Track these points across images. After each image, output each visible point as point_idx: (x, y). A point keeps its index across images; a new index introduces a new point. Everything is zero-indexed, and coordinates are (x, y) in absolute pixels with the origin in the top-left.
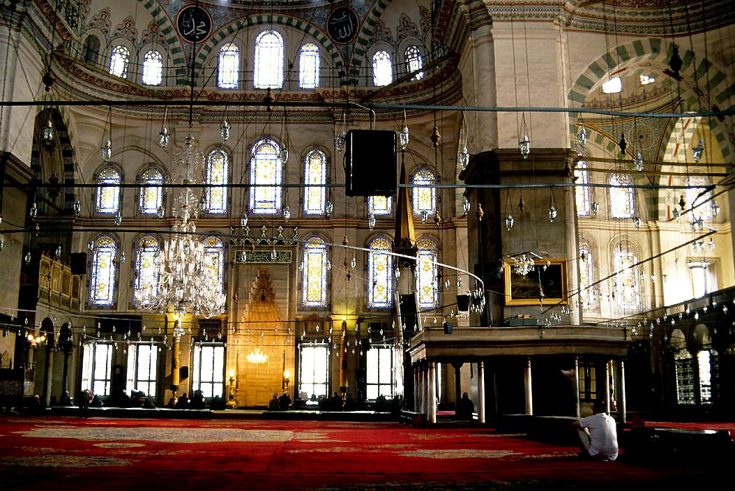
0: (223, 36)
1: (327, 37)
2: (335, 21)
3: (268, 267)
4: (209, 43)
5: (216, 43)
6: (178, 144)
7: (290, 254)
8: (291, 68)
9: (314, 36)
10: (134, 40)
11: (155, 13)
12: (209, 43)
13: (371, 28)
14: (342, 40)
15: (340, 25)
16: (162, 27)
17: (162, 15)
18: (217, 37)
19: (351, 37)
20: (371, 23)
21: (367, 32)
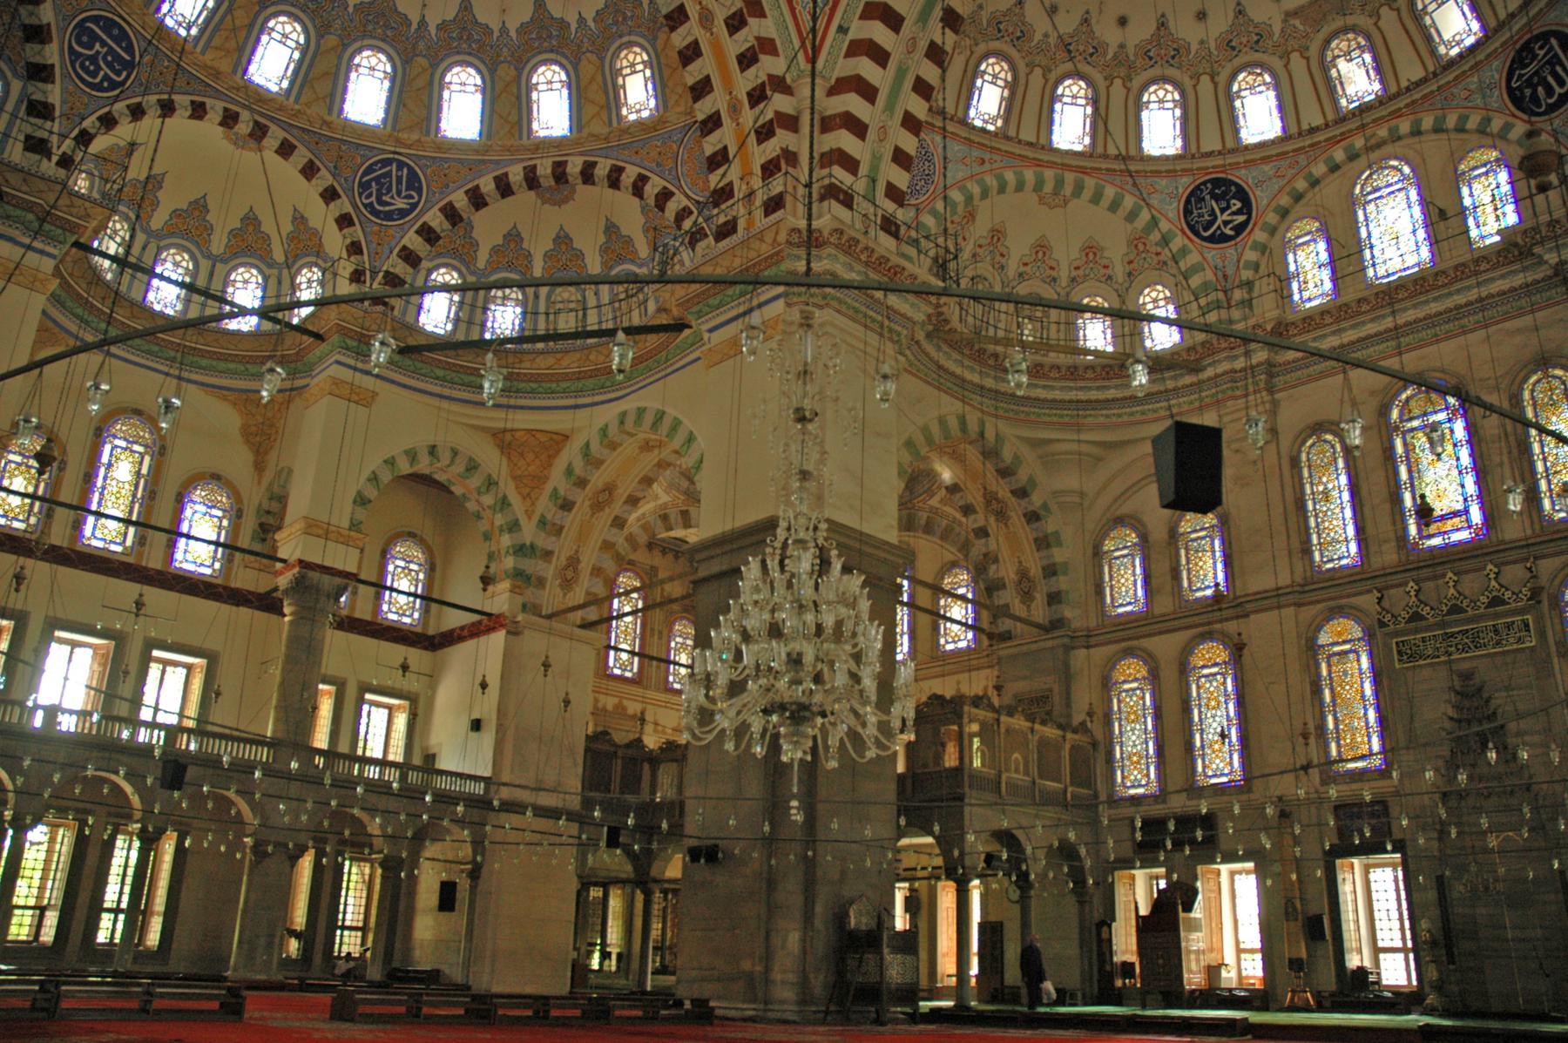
0: (1284, 213)
1: (1510, 119)
3: (1475, 663)
5: (1273, 231)
7: (1527, 625)
8: (1443, 217)
9: (1482, 131)
18: (1272, 218)
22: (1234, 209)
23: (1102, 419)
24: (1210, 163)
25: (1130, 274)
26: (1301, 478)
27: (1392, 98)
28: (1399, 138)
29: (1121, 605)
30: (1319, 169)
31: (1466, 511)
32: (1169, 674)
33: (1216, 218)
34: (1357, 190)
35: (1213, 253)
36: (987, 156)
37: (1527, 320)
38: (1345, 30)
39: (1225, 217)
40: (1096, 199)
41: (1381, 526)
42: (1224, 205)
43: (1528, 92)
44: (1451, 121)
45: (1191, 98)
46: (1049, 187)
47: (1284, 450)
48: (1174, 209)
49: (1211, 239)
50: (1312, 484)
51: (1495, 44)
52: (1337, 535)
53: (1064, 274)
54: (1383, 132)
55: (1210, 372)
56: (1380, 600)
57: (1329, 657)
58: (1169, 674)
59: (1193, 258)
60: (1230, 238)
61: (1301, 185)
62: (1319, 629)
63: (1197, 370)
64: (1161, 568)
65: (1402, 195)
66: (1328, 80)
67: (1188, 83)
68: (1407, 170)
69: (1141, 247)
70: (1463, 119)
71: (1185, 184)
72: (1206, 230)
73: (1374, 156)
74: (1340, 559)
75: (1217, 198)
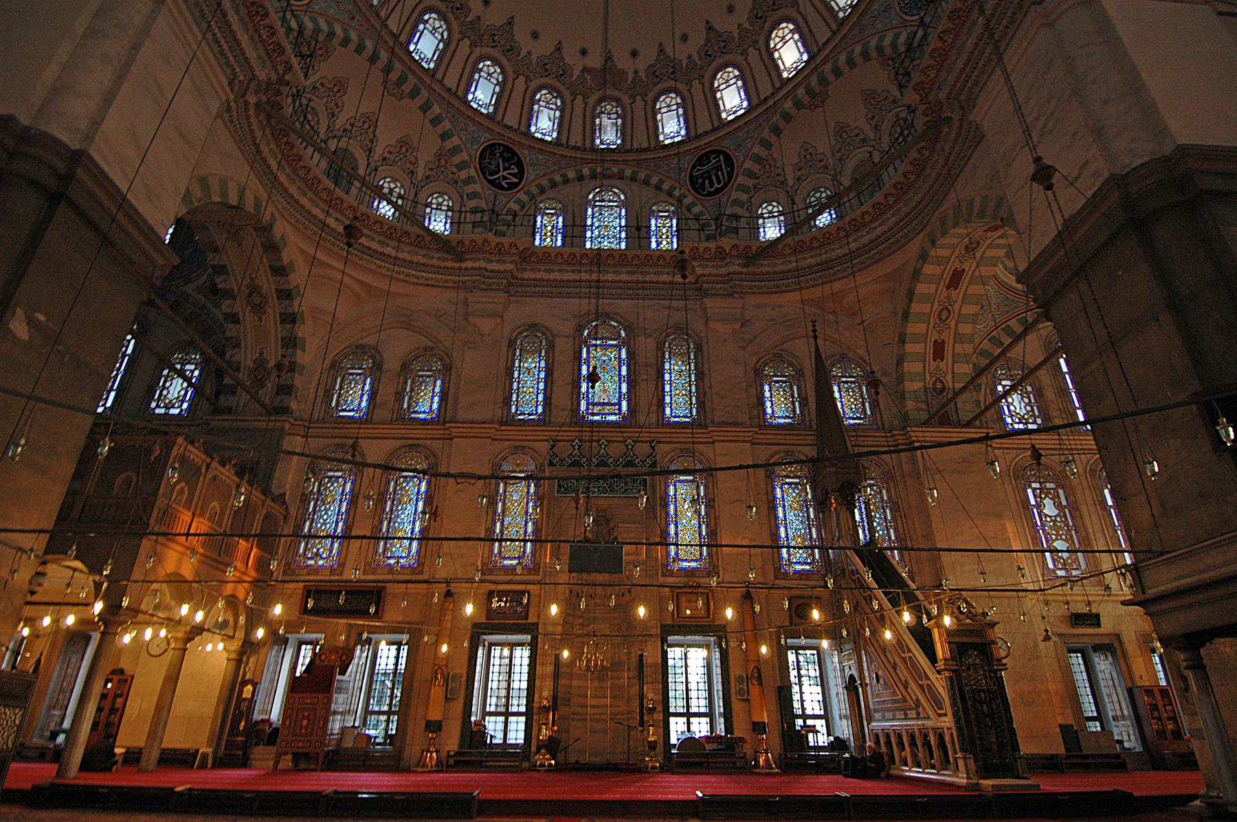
0: (542, 190)
4: (523, 197)
5: (532, 197)
6: (471, 319)
8: (638, 230)
9: (669, 193)
10: (412, 172)
11: (445, 136)
12: (523, 197)
13: (756, 168)
14: (710, 194)
16: (456, 159)
17: (455, 141)
18: (534, 190)
19: (726, 185)
20: (758, 159)
21: (749, 174)
23: (374, 267)
24: (508, 134)
28: (622, 178)
29: (344, 410)
30: (571, 174)
31: (619, 404)
34: (591, 197)
35: (490, 192)
36: (358, 17)
41: (561, 399)
44: (654, 180)
45: (509, 86)
47: (507, 331)
48: (476, 150)
49: (492, 183)
54: (615, 170)
55: (469, 264)
56: (553, 447)
60: (502, 188)
61: (558, 178)
64: (387, 390)
67: (511, 75)
68: (622, 197)
69: (443, 162)
71: (485, 138)
72: (491, 175)
73: (606, 182)
74: (530, 414)
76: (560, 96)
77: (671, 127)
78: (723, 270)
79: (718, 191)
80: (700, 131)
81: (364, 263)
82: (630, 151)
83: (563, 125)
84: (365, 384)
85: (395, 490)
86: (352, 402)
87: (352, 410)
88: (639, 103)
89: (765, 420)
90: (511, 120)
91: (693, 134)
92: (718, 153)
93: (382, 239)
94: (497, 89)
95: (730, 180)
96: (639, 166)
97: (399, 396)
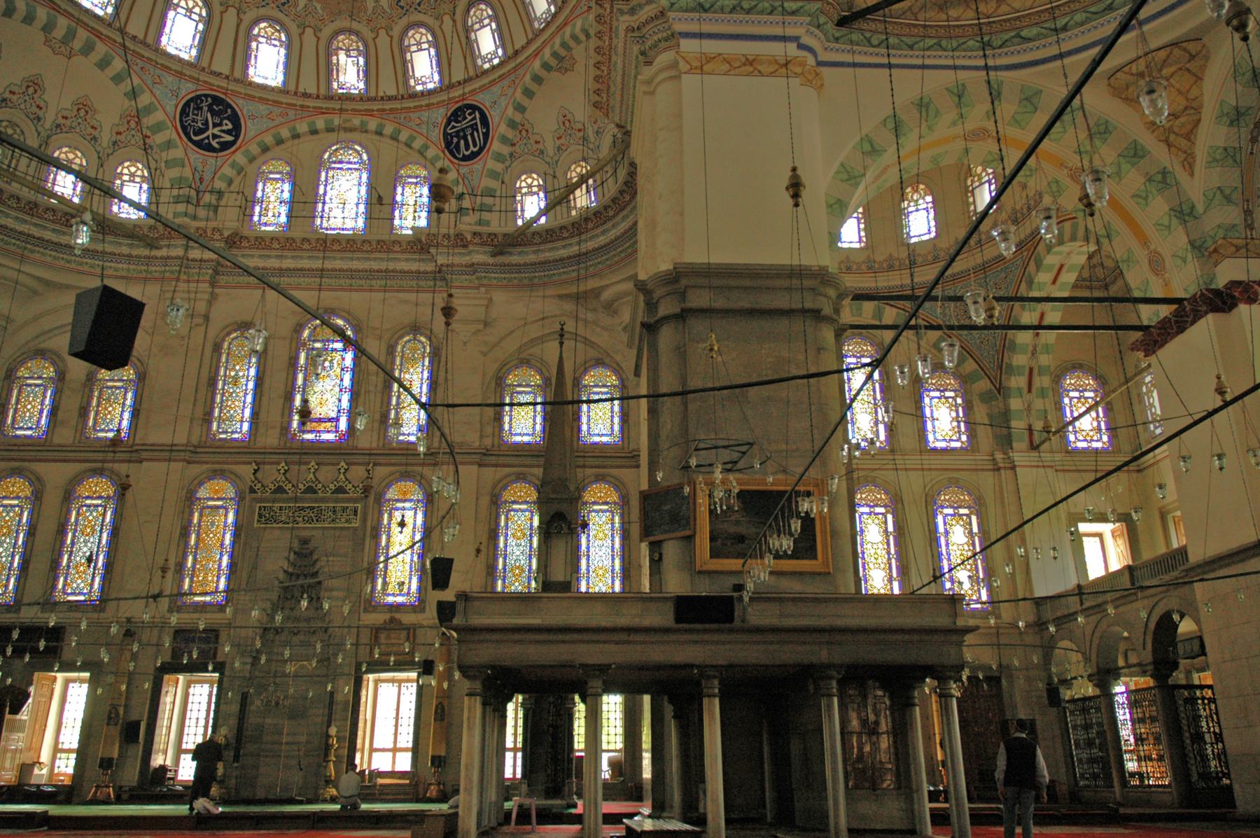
0: (265, 149)
2: (454, 127)
3: (314, 533)
7: (356, 511)
9: (421, 153)
13: (510, 134)
14: (465, 158)
15: (461, 134)
18: (254, 149)
19: (482, 149)
20: (512, 124)
22: (225, 128)
24: (215, 81)
25: (115, 143)
26: (219, 361)
27: (369, 99)
28: (366, 131)
30: (302, 127)
31: (337, 419)
32: (52, 498)
33: (207, 129)
34: (326, 156)
35: (196, 156)
37: (412, 297)
38: (350, 31)
39: (216, 131)
40: (103, 64)
41: (272, 414)
42: (217, 121)
43: (455, 140)
44: (404, 136)
46: (59, 33)
47: (212, 333)
49: (199, 144)
50: (226, 368)
51: (444, 97)
52: (236, 414)
53: (50, 119)
54: (356, 121)
55: (163, 252)
56: (256, 471)
57: (203, 508)
58: (52, 498)
59: (177, 153)
61: (285, 133)
62: (201, 484)
63: (152, 246)
64: (71, 404)
65: (356, 174)
66: (329, 62)
68: (365, 157)
70: (412, 138)
71: (188, 90)
72: (196, 135)
73: (343, 135)
75: (213, 113)
76: (284, 28)
77: (423, 68)
78: (466, 260)
79: (474, 155)
80: (454, 80)
81: (37, 256)
82: (375, 99)
83: (292, 66)
84: (45, 397)
85: (77, 520)
86: (30, 417)
87: (30, 428)
88: (383, 38)
89: (501, 437)
90: (222, 65)
91: (447, 82)
92: (474, 108)
93: (57, 227)
94: (201, 27)
95: (485, 143)
96: (380, 117)
97: (84, 412)
